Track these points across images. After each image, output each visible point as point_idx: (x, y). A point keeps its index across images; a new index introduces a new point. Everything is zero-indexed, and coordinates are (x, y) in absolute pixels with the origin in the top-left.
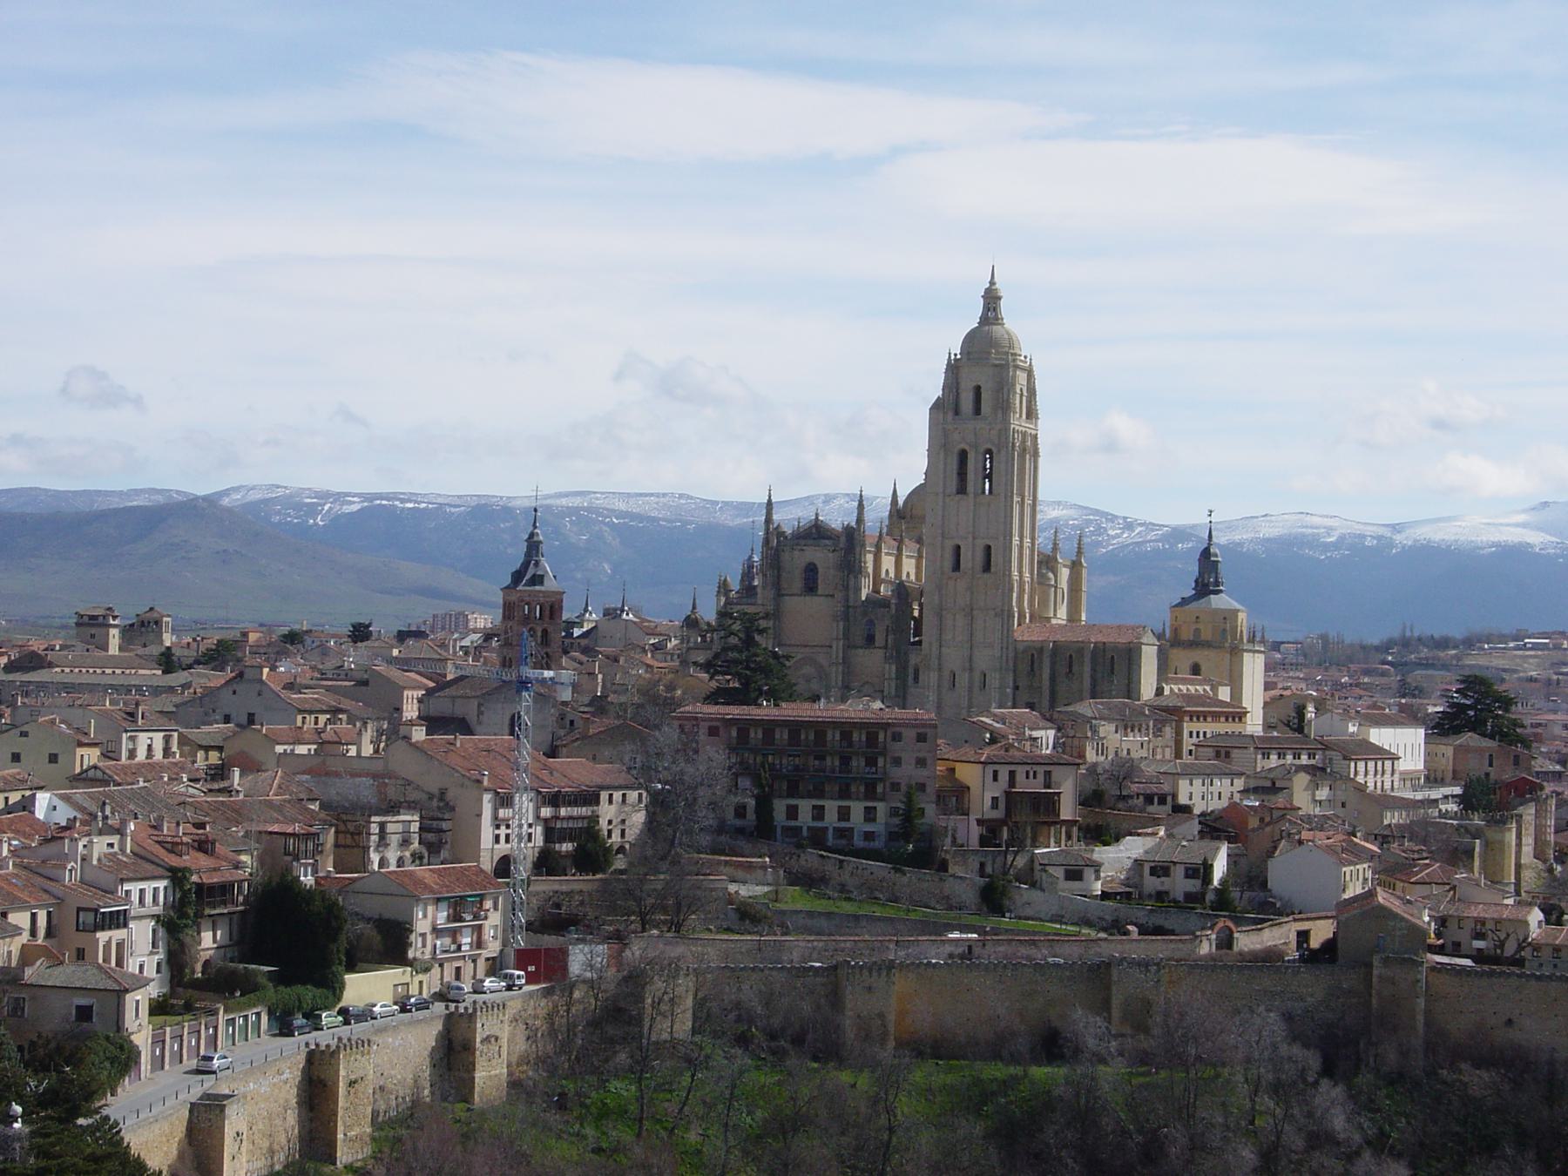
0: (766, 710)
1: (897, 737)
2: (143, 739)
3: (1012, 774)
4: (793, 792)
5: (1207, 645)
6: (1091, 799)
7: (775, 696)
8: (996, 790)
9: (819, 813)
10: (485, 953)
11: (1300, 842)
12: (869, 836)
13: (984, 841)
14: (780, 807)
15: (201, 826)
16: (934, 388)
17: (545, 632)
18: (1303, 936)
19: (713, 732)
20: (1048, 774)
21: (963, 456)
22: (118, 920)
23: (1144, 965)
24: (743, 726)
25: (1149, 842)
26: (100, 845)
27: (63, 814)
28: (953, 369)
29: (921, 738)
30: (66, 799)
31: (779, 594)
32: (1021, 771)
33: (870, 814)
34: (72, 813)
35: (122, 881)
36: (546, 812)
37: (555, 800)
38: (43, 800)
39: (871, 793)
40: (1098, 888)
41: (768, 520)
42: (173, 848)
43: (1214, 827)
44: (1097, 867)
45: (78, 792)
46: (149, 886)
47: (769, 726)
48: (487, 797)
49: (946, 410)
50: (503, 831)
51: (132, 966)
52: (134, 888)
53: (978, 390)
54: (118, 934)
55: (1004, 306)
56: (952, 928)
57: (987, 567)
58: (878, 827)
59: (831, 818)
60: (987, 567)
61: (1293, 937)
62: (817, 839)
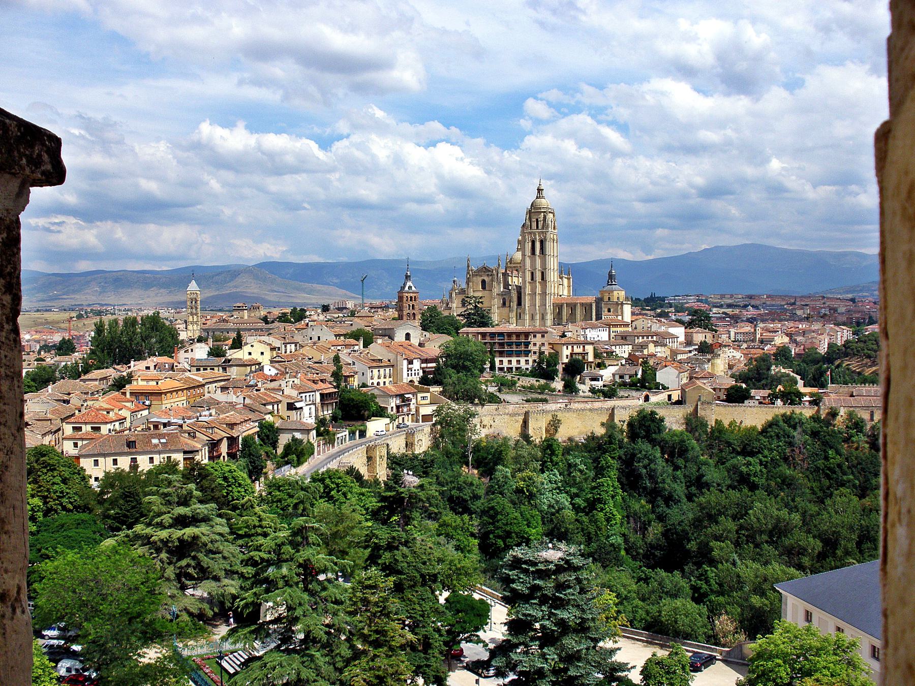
2: (288, 346)
3: (573, 347)
6: (596, 355)
9: (510, 362)
10: (412, 413)
11: (666, 366)
12: (527, 369)
14: (497, 360)
17: (413, 305)
18: (670, 396)
20: (584, 347)
23: (624, 408)
25: (617, 368)
32: (575, 347)
33: (527, 361)
34: (277, 372)
35: (300, 393)
44: (602, 376)
46: (308, 394)
48: (405, 362)
50: (410, 372)
53: (537, 220)
58: (529, 366)
61: (667, 397)
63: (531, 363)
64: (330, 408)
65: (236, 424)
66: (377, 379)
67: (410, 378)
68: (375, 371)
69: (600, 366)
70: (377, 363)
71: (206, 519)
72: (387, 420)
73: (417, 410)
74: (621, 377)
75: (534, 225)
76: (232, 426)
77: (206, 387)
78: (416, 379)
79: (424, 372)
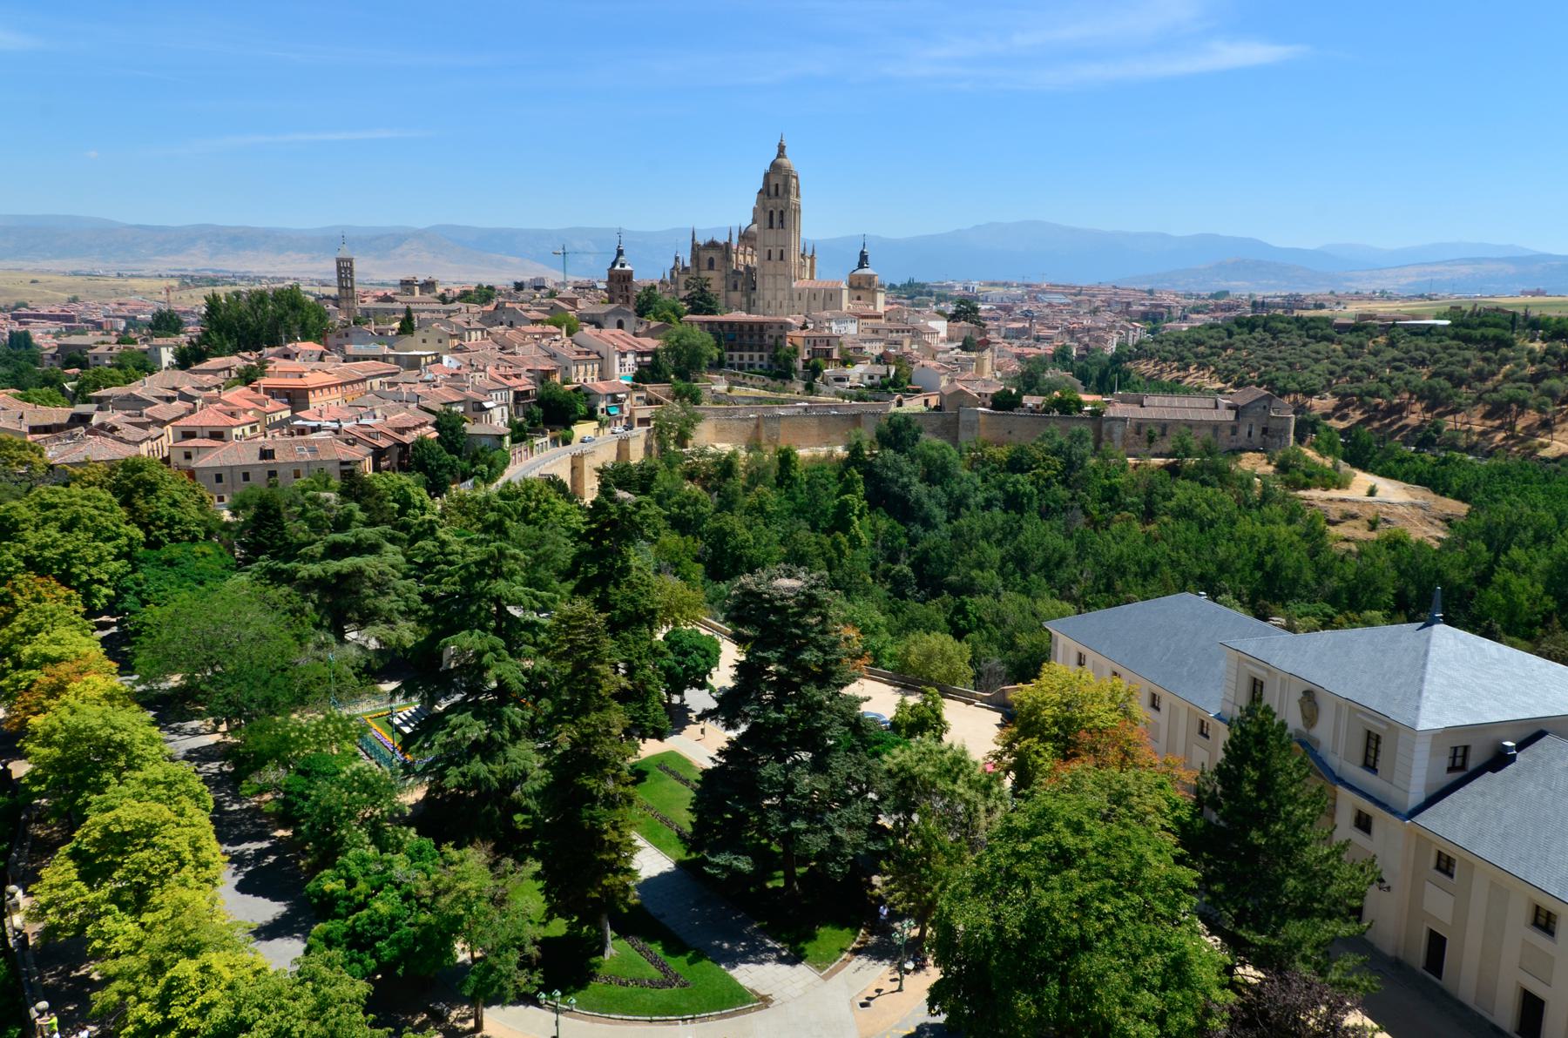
2: (473, 333)
4: (732, 349)
7: (713, 312)
9: (741, 358)
12: (761, 366)
13: (804, 367)
14: (726, 355)
16: (760, 186)
18: (926, 402)
21: (771, 213)
24: (709, 323)
25: (866, 366)
27: (455, 365)
28: (767, 176)
29: (781, 327)
31: (699, 270)
33: (761, 358)
36: (639, 359)
37: (642, 354)
38: (446, 359)
40: (848, 384)
41: (693, 240)
42: (505, 377)
43: (882, 359)
45: (458, 355)
47: (721, 324)
48: (617, 356)
49: (765, 193)
55: (787, 152)
57: (782, 258)
60: (782, 258)
62: (741, 367)
63: (766, 358)
65: (409, 429)
66: (584, 376)
68: (582, 368)
69: (846, 361)
71: (374, 549)
72: (595, 424)
73: (631, 413)
74: (871, 377)
75: (772, 190)
76: (402, 431)
77: (368, 382)
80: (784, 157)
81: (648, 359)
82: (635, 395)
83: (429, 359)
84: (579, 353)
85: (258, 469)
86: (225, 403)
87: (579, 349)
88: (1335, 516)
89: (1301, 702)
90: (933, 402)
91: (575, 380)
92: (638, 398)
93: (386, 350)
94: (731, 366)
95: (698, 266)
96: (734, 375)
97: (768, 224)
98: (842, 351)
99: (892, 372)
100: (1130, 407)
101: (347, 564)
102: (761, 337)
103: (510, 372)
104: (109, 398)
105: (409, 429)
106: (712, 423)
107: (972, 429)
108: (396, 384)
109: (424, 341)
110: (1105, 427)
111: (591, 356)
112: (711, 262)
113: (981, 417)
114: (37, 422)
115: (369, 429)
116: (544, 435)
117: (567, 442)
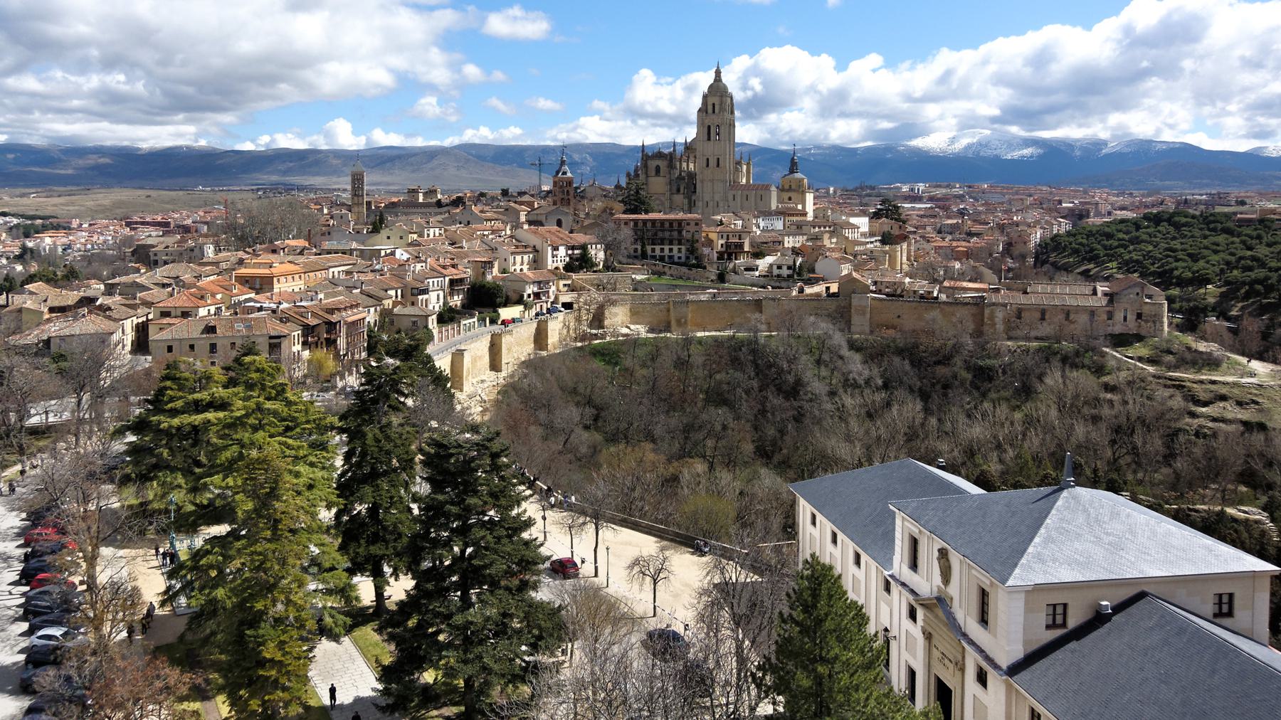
0: (643, 216)
1: (688, 224)
2: (432, 230)
5: (794, 191)
7: (647, 212)
8: (721, 242)
9: (662, 250)
12: (680, 258)
13: (718, 259)
14: (649, 248)
15: (453, 259)
18: (828, 288)
19: (626, 224)
22: (425, 291)
24: (636, 222)
25: (775, 258)
26: (419, 266)
27: (406, 256)
28: (705, 97)
29: (697, 224)
30: (407, 251)
32: (731, 235)
33: (680, 251)
36: (570, 252)
37: (573, 248)
38: (398, 252)
39: (680, 243)
40: (757, 273)
42: (444, 267)
43: (796, 252)
46: (436, 280)
47: (645, 222)
48: (550, 248)
51: (431, 307)
52: (431, 281)
54: (425, 297)
56: (709, 288)
57: (718, 165)
58: (683, 255)
59: (667, 252)
60: (718, 165)
62: (662, 259)
64: (461, 292)
65: (339, 310)
66: (520, 264)
67: (555, 265)
68: (518, 258)
69: (758, 255)
70: (521, 247)
72: (521, 308)
73: (556, 298)
74: (779, 267)
75: (710, 108)
76: (331, 311)
77: (331, 270)
78: (561, 265)
79: (571, 258)
80: (720, 80)
81: (576, 252)
82: (562, 283)
83: (388, 251)
84: (517, 247)
85: (202, 342)
86: (199, 289)
87: (518, 244)
88: (1203, 396)
89: (939, 559)
90: (834, 288)
91: (512, 269)
92: (565, 285)
93: (354, 245)
94: (654, 257)
95: (646, 173)
96: (655, 265)
97: (706, 137)
98: (752, 245)
99: (798, 264)
100: (1015, 293)
101: (198, 419)
102: (680, 232)
103: (448, 262)
104: (118, 284)
105: (339, 310)
106: (628, 307)
107: (864, 314)
108: (352, 273)
109: (389, 238)
110: (987, 311)
111: (529, 250)
112: (658, 169)
113: (873, 302)
114: (56, 304)
115: (303, 310)
116: (472, 316)
117: (493, 322)
